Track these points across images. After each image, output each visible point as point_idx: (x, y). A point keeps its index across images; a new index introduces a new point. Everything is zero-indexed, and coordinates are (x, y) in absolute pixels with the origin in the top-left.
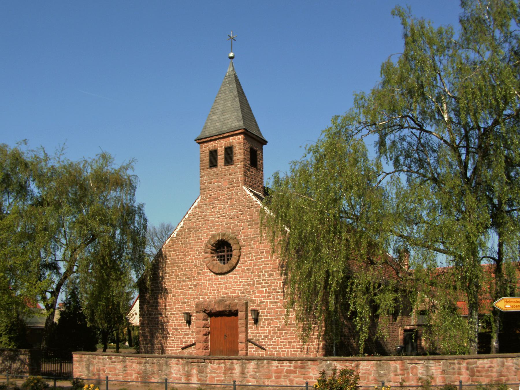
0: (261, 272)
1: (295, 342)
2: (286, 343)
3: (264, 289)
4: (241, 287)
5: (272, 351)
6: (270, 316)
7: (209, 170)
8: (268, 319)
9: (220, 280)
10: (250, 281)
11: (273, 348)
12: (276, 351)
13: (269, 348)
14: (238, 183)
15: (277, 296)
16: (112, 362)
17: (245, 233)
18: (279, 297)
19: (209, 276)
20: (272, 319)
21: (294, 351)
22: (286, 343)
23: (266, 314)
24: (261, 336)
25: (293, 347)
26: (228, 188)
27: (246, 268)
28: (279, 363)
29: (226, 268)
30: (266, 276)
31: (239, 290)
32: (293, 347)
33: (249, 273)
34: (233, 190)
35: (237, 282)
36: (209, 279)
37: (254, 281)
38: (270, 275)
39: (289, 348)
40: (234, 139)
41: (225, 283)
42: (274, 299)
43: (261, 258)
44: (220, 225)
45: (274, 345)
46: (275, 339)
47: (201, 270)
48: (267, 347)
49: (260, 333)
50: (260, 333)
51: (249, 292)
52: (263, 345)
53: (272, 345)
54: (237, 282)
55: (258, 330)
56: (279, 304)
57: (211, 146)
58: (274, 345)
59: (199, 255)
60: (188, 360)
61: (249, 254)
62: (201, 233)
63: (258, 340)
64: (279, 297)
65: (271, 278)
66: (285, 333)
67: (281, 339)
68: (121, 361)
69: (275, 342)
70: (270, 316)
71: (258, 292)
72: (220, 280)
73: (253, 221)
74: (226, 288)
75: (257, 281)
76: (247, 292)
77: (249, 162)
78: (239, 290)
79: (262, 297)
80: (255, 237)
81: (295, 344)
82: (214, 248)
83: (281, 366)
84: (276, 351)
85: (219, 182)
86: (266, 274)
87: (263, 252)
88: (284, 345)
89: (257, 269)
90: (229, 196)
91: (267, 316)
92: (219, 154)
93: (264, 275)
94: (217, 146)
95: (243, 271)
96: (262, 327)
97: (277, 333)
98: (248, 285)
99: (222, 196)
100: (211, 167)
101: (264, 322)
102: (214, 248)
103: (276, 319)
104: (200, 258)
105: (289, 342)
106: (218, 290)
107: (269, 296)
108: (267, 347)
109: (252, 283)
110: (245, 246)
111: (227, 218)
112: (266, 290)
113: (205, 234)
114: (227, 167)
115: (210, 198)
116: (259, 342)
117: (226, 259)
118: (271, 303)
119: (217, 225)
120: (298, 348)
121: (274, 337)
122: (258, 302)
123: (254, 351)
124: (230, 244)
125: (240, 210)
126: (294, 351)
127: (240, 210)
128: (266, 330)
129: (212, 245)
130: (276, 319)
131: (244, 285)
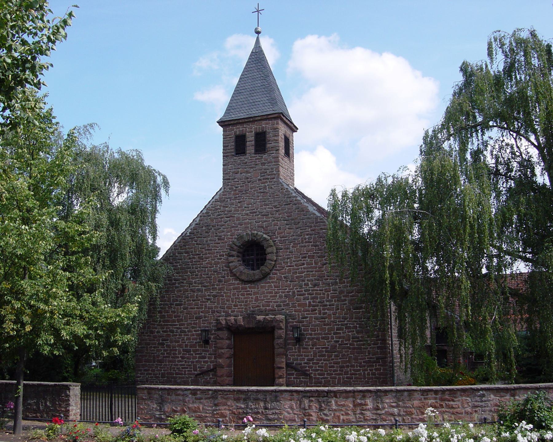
0: (303, 281)
1: (348, 366)
2: (337, 367)
3: (307, 302)
4: (277, 299)
5: (318, 378)
6: (315, 334)
7: (235, 158)
8: (313, 338)
9: (248, 289)
10: (288, 292)
11: (319, 374)
12: (323, 378)
13: (315, 375)
14: (272, 175)
15: (324, 309)
16: (196, 399)
17: (281, 233)
18: (326, 311)
19: (234, 284)
20: (318, 339)
21: (347, 378)
22: (337, 367)
23: (310, 332)
24: (303, 359)
25: (346, 373)
26: (260, 180)
27: (283, 276)
28: (422, 395)
29: (257, 273)
30: (310, 286)
31: (274, 302)
32: (346, 373)
33: (287, 281)
34: (267, 182)
35: (271, 293)
36: (234, 289)
37: (294, 292)
38: (315, 285)
39: (342, 374)
40: (267, 124)
41: (255, 293)
42: (320, 314)
43: (303, 264)
44: (248, 223)
45: (322, 370)
46: (322, 363)
47: (224, 277)
48: (312, 373)
49: (302, 356)
50: (302, 356)
51: (288, 305)
52: (306, 370)
53: (318, 370)
54: (271, 293)
55: (299, 352)
56: (327, 320)
57: (238, 130)
58: (322, 370)
59: (221, 259)
60: (306, 395)
61: (288, 259)
62: (223, 231)
63: (301, 364)
64: (326, 311)
65: (316, 288)
66: (336, 356)
67: (331, 363)
68: (209, 398)
69: (322, 367)
70: (315, 334)
71: (299, 305)
72: (248, 289)
73: (292, 220)
74: (257, 300)
75: (298, 291)
76: (284, 305)
77: (284, 152)
78: (274, 302)
79: (304, 311)
80: (294, 239)
81: (349, 370)
82: (241, 250)
83: (425, 399)
84: (323, 378)
85: (247, 172)
86: (309, 283)
87: (305, 257)
88: (334, 371)
89: (297, 277)
90: (260, 189)
91: (311, 334)
92: (248, 140)
93: (307, 285)
94: (246, 131)
95: (280, 279)
96: (304, 348)
97: (324, 355)
98: (286, 296)
99: (251, 189)
100: (236, 154)
101: (307, 342)
102: (241, 250)
103: (323, 338)
104: (222, 262)
105: (341, 367)
106: (246, 302)
107: (313, 310)
108: (312, 373)
109: (291, 293)
110: (282, 249)
111: (258, 215)
112: (309, 302)
113: (229, 233)
114: (258, 156)
115: (235, 190)
116: (302, 367)
117: (255, 264)
118: (316, 318)
119: (245, 223)
120: (352, 374)
121: (321, 360)
122: (299, 317)
123: (294, 378)
124: (263, 246)
125: (275, 207)
126: (347, 378)
127: (275, 207)
128: (310, 352)
129: (239, 247)
130: (323, 338)
131: (281, 297)
